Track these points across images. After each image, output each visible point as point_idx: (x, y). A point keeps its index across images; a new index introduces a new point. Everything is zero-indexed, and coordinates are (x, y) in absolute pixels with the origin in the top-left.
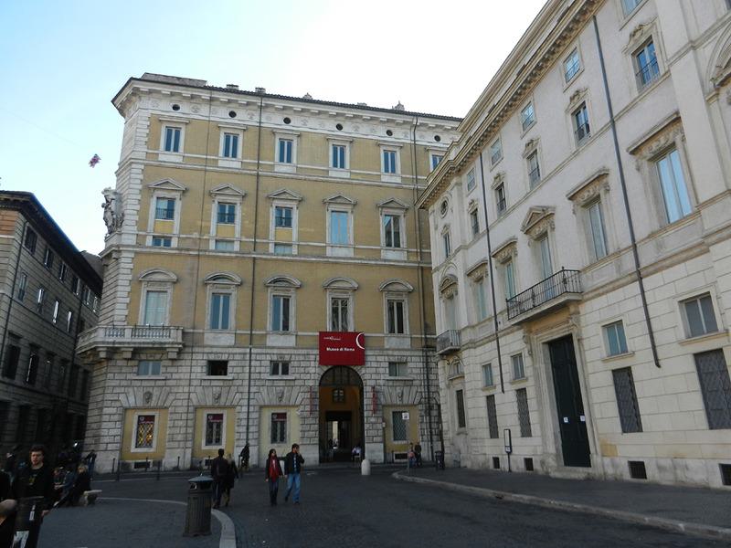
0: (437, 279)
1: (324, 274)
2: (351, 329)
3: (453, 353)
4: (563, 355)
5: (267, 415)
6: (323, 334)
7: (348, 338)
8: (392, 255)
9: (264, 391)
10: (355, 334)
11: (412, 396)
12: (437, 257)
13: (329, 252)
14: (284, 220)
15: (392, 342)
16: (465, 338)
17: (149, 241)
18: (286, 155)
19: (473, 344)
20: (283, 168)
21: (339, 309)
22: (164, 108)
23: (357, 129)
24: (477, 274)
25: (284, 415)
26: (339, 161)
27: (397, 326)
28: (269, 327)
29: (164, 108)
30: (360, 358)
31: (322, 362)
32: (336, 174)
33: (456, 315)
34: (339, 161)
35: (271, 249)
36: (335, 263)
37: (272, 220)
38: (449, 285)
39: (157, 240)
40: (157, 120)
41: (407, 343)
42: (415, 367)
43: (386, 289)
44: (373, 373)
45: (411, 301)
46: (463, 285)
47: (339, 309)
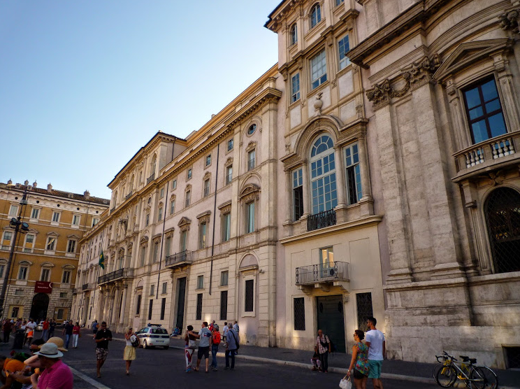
1: (42, 261)
2: (48, 281)
3: (76, 294)
4: (182, 284)
5: (12, 308)
6: (37, 282)
7: (46, 284)
8: (69, 255)
9: (12, 300)
13: (45, 253)
15: (63, 286)
16: (79, 290)
18: (35, 216)
19: (79, 293)
21: (46, 272)
25: (18, 308)
28: (18, 278)
30: (50, 291)
31: (35, 292)
35: (23, 250)
36: (47, 257)
43: (64, 268)
44: (54, 297)
47: (46, 272)
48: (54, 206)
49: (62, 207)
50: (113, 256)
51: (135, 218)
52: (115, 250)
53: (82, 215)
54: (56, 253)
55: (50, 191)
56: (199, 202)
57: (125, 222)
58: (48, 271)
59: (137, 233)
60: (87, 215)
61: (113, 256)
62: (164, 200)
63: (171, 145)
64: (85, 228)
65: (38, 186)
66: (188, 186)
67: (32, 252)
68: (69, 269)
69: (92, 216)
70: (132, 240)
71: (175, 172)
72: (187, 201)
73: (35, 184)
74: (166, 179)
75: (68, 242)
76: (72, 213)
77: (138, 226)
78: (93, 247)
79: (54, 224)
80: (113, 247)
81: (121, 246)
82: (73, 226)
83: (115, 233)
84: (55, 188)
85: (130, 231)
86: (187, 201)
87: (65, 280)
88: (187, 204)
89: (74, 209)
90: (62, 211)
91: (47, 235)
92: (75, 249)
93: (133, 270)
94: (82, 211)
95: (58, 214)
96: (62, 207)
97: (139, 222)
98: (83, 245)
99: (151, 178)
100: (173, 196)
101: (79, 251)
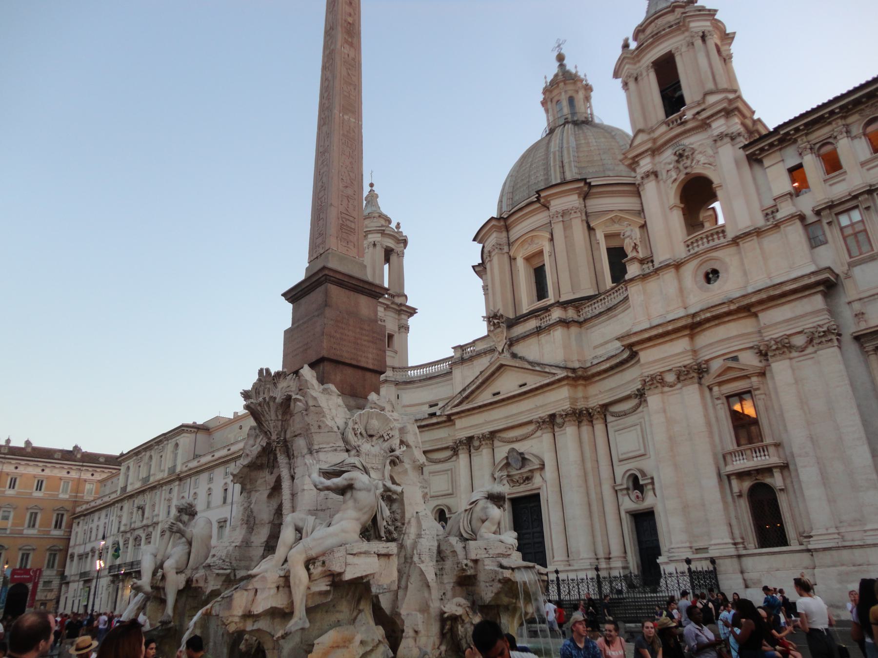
0: (70, 551)
2: (28, 567)
3: (68, 583)
8: (56, 533)
10: (30, 569)
11: (51, 596)
12: (72, 543)
13: (25, 532)
16: (72, 578)
18: (13, 485)
19: (74, 581)
20: (10, 492)
21: (25, 557)
24: (80, 557)
27: (51, 565)
32: (38, 494)
33: (72, 569)
34: (39, 487)
36: (28, 537)
38: (72, 556)
41: (55, 572)
42: (56, 583)
45: (60, 553)
46: (76, 558)
47: (25, 557)
48: (37, 471)
49: (47, 472)
50: (126, 542)
51: (154, 505)
52: (128, 535)
53: (73, 480)
54: (39, 531)
55: (29, 450)
56: (218, 507)
57: (141, 508)
58: (28, 555)
59: (157, 523)
60: (79, 479)
61: (126, 542)
62: (186, 495)
63: (193, 435)
64: (76, 497)
65: (13, 444)
66: (209, 489)
68: (55, 550)
70: (151, 529)
71: (198, 472)
72: (209, 503)
74: (189, 476)
76: (61, 479)
77: (158, 515)
78: (94, 526)
79: (38, 494)
80: (125, 532)
81: (137, 533)
82: (61, 496)
83: (127, 515)
84: (36, 444)
85: (148, 518)
86: (209, 503)
87: (51, 565)
88: (208, 506)
89: (63, 474)
90: (48, 478)
91: (27, 509)
92: (64, 524)
94: (74, 475)
97: (159, 511)
98: (77, 521)
99: (172, 470)
100: (195, 493)
101: (70, 527)
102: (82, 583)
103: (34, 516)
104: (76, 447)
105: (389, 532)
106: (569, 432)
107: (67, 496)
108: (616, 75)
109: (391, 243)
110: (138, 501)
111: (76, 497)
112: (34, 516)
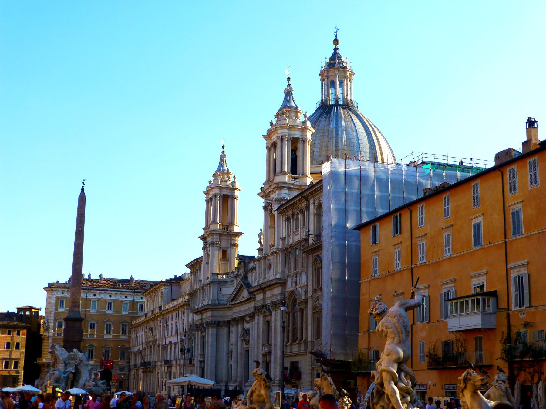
8: (123, 337)
14: (92, 327)
17: (56, 335)
22: (59, 294)
23: (116, 296)
26: (110, 308)
29: (59, 294)
30: (112, 367)
32: (109, 312)
34: (110, 308)
36: (107, 340)
37: (89, 327)
39: (58, 334)
40: (57, 298)
48: (107, 297)
54: (113, 336)
57: (151, 329)
63: (170, 287)
64: (133, 313)
67: (95, 336)
69: (137, 302)
73: (89, 276)
75: (121, 326)
76: (122, 301)
77: (156, 335)
79: (109, 312)
82: (124, 313)
89: (123, 298)
90: (114, 301)
93: (155, 362)
94: (130, 298)
95: (111, 304)
96: (113, 297)
102: (166, 368)
103: (109, 327)
104: (131, 278)
105: (37, 385)
106: (210, 332)
107: (127, 313)
108: (206, 193)
109: (226, 192)
110: (151, 325)
111: (133, 313)
112: (109, 327)
